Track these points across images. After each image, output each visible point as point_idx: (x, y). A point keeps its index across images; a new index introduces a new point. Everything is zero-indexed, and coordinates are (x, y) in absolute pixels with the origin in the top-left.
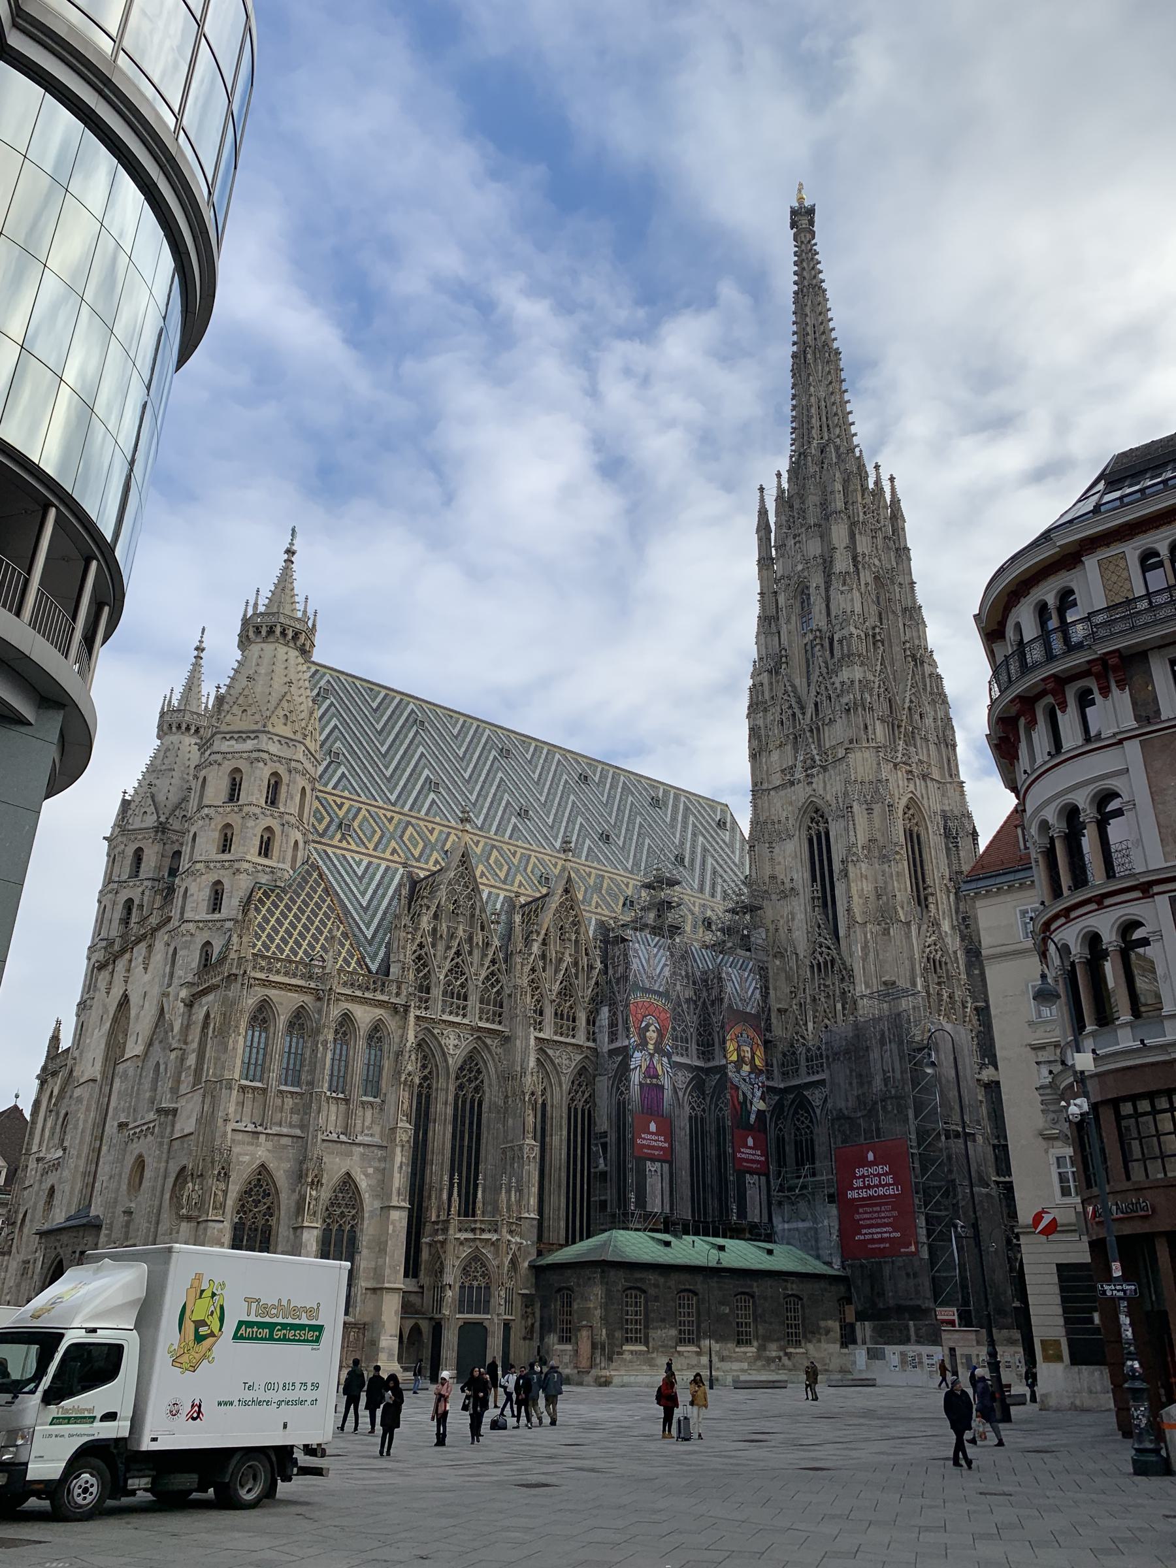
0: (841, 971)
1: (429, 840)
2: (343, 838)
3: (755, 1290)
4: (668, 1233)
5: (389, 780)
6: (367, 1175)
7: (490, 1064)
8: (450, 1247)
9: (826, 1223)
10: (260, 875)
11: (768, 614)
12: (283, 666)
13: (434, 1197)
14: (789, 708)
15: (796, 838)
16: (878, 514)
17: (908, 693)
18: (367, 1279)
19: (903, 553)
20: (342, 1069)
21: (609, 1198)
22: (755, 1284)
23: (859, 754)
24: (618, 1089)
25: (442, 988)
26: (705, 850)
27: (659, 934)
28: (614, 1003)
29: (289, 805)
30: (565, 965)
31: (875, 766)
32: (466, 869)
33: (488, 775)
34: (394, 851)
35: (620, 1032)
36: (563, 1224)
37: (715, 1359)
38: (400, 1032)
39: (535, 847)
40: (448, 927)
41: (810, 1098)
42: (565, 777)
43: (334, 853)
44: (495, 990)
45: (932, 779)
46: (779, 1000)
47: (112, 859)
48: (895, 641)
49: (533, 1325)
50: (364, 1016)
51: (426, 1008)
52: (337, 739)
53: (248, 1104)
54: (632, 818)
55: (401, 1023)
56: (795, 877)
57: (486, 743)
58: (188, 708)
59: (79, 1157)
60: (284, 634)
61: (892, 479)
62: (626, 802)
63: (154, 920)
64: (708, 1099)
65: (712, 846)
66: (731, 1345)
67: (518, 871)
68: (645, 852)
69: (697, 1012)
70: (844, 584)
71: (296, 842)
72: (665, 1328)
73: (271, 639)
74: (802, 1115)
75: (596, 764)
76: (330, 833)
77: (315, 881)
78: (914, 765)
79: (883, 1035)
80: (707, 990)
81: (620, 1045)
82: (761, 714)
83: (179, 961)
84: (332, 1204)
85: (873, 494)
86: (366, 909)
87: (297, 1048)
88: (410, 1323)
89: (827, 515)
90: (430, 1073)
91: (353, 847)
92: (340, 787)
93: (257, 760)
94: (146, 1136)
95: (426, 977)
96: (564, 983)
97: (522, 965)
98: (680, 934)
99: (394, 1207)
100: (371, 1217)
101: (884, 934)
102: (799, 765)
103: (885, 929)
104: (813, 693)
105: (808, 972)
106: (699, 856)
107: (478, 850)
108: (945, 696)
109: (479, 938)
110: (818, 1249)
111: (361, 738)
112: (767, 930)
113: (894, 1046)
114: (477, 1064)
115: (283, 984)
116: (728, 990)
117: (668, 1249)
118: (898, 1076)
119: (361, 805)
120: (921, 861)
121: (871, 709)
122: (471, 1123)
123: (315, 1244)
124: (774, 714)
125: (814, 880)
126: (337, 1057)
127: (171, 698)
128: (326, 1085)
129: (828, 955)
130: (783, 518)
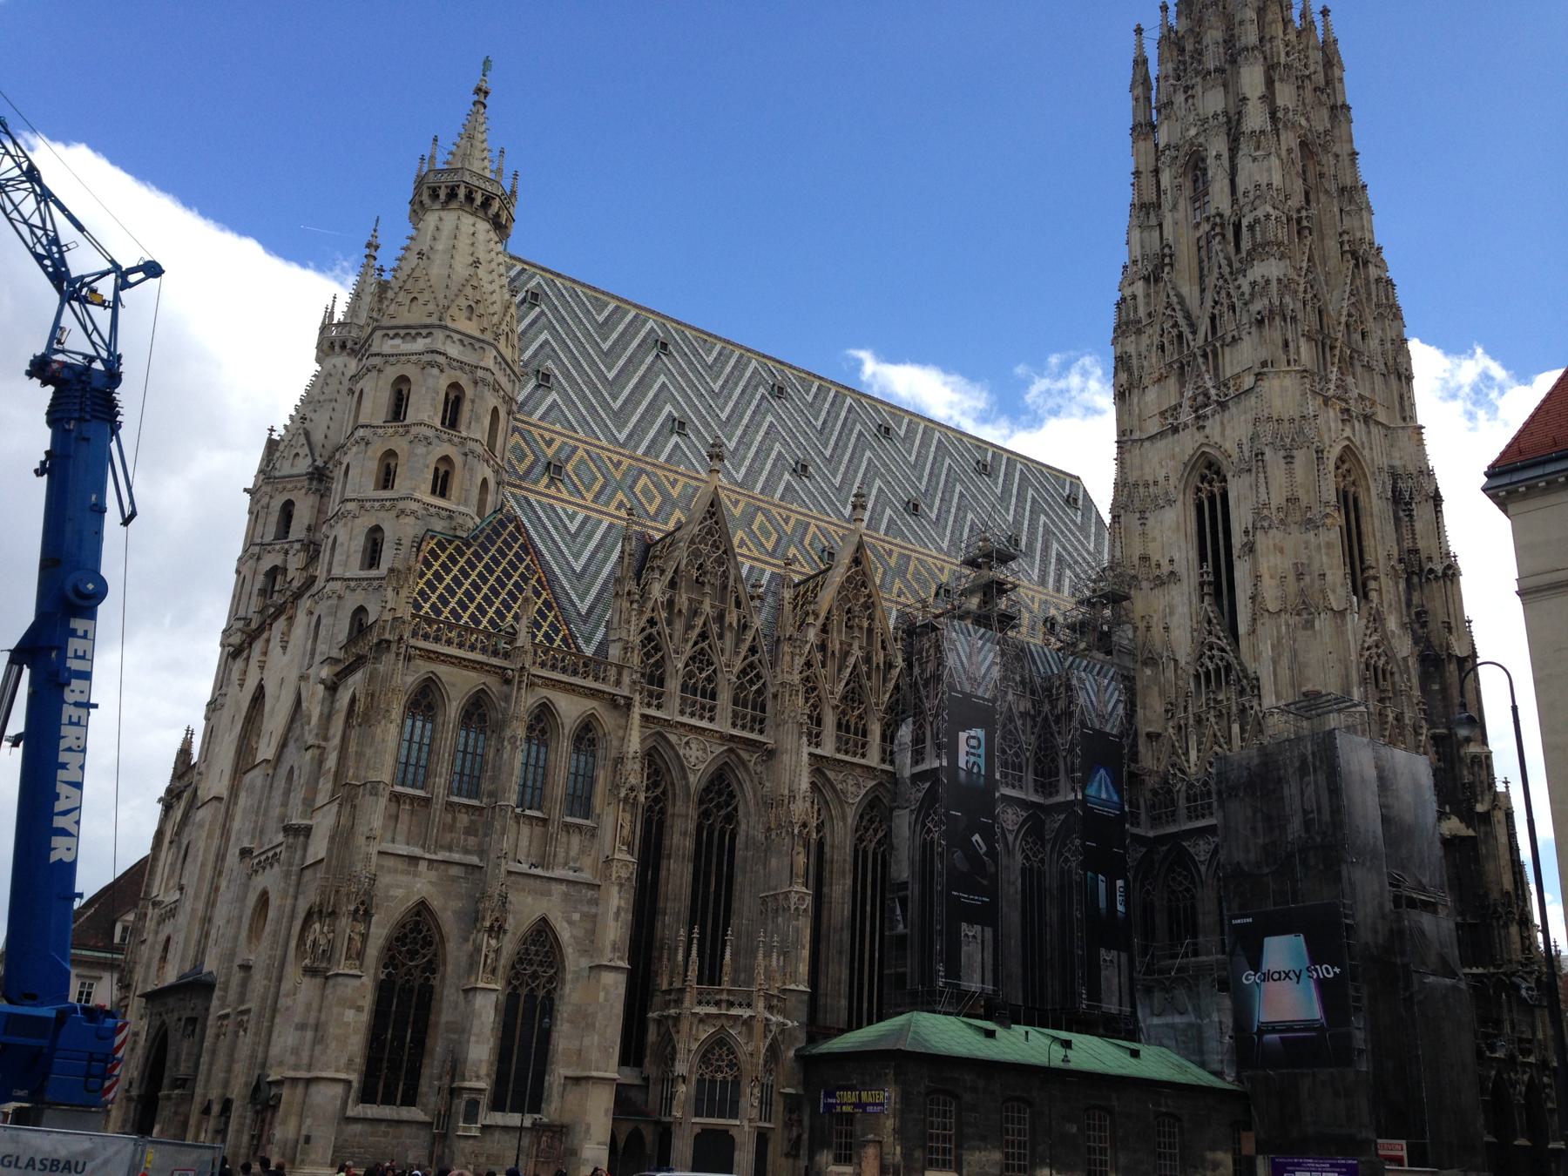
0: (1239, 680)
3: (1116, 1104)
4: (990, 1020)
6: (570, 923)
7: (747, 786)
8: (684, 1026)
9: (1215, 1017)
10: (434, 520)
11: (1146, 199)
13: (665, 956)
14: (1173, 327)
15: (1179, 504)
16: (1307, 57)
17: (1345, 304)
19: (1340, 111)
20: (539, 778)
21: (909, 970)
23: (1276, 383)
24: (924, 825)
25: (680, 681)
26: (1047, 530)
27: (988, 626)
28: (921, 713)
29: (475, 428)
30: (852, 660)
31: (1298, 397)
32: (716, 523)
34: (620, 505)
35: (928, 748)
36: (844, 1003)
38: (621, 733)
39: (815, 513)
40: (690, 600)
41: (1192, 850)
42: (858, 427)
43: (538, 502)
44: (754, 688)
45: (1377, 423)
46: (1148, 722)
47: (255, 514)
48: (1329, 232)
49: (799, 1137)
50: (570, 709)
51: (659, 707)
52: (549, 357)
53: (404, 817)
55: (623, 722)
57: (750, 378)
58: (355, 321)
59: (196, 897)
61: (1325, 12)
63: (296, 584)
64: (1048, 848)
65: (1057, 527)
67: (791, 541)
68: (967, 530)
69: (1036, 730)
70: (1258, 148)
71: (485, 482)
72: (985, 1150)
73: (454, 205)
74: (1180, 874)
76: (532, 476)
77: (511, 534)
78: (1352, 402)
79: (1304, 761)
80: (1050, 702)
81: (928, 767)
82: (1133, 337)
83: (322, 632)
84: (521, 961)
85: (1299, 34)
86: (580, 577)
87: (476, 747)
88: (626, 1128)
89: (1234, 54)
90: (664, 793)
91: (565, 495)
93: (431, 364)
94: (272, 865)
95: (660, 664)
96: (852, 684)
97: (793, 655)
98: (1014, 627)
99: (606, 966)
100: (576, 980)
101: (1305, 628)
102: (1186, 403)
103: (1307, 621)
104: (1209, 303)
105: (1192, 685)
106: (1040, 539)
107: (737, 512)
108: (1398, 309)
109: (732, 618)
110: (1201, 1052)
112: (1136, 629)
113: (1322, 778)
114: (729, 785)
115: (456, 657)
116: (1081, 701)
117: (989, 1042)
118: (1326, 817)
119: (577, 444)
120: (1359, 534)
121: (1294, 319)
122: (719, 864)
123: (492, 1013)
124: (1150, 336)
125: (1202, 558)
126: (532, 761)
128: (512, 799)
129: (1222, 659)
130: (1170, 66)
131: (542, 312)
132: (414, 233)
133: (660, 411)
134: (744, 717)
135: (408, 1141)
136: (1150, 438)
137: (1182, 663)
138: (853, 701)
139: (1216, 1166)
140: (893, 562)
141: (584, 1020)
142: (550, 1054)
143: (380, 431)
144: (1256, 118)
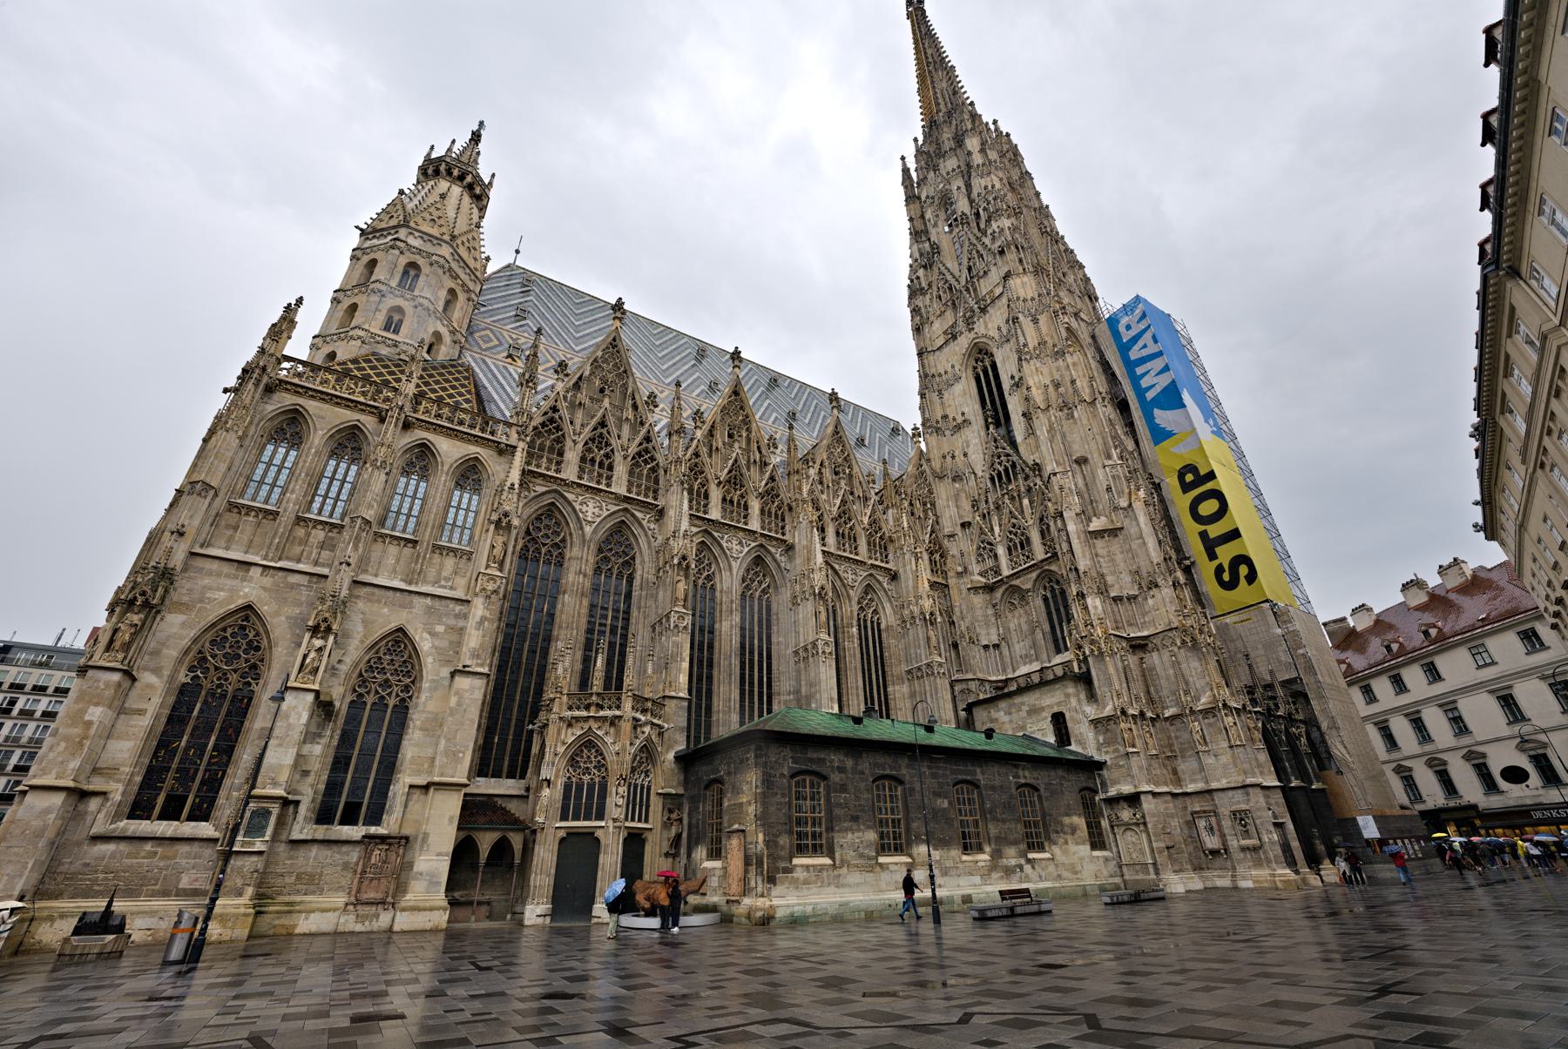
2: (510, 356)
3: (980, 777)
6: (432, 634)
7: (642, 541)
8: (552, 730)
11: (919, 229)
18: (418, 772)
22: (978, 770)
23: (1018, 281)
37: (936, 872)
49: (679, 836)
56: (966, 410)
66: (955, 853)
72: (859, 830)
93: (392, 247)
100: (434, 689)
104: (965, 261)
105: (989, 485)
134: (639, 486)
135: (184, 862)
136: (940, 348)
137: (980, 474)
138: (735, 484)
139: (1074, 830)
141: (435, 725)
142: (398, 763)
144: (977, 159)
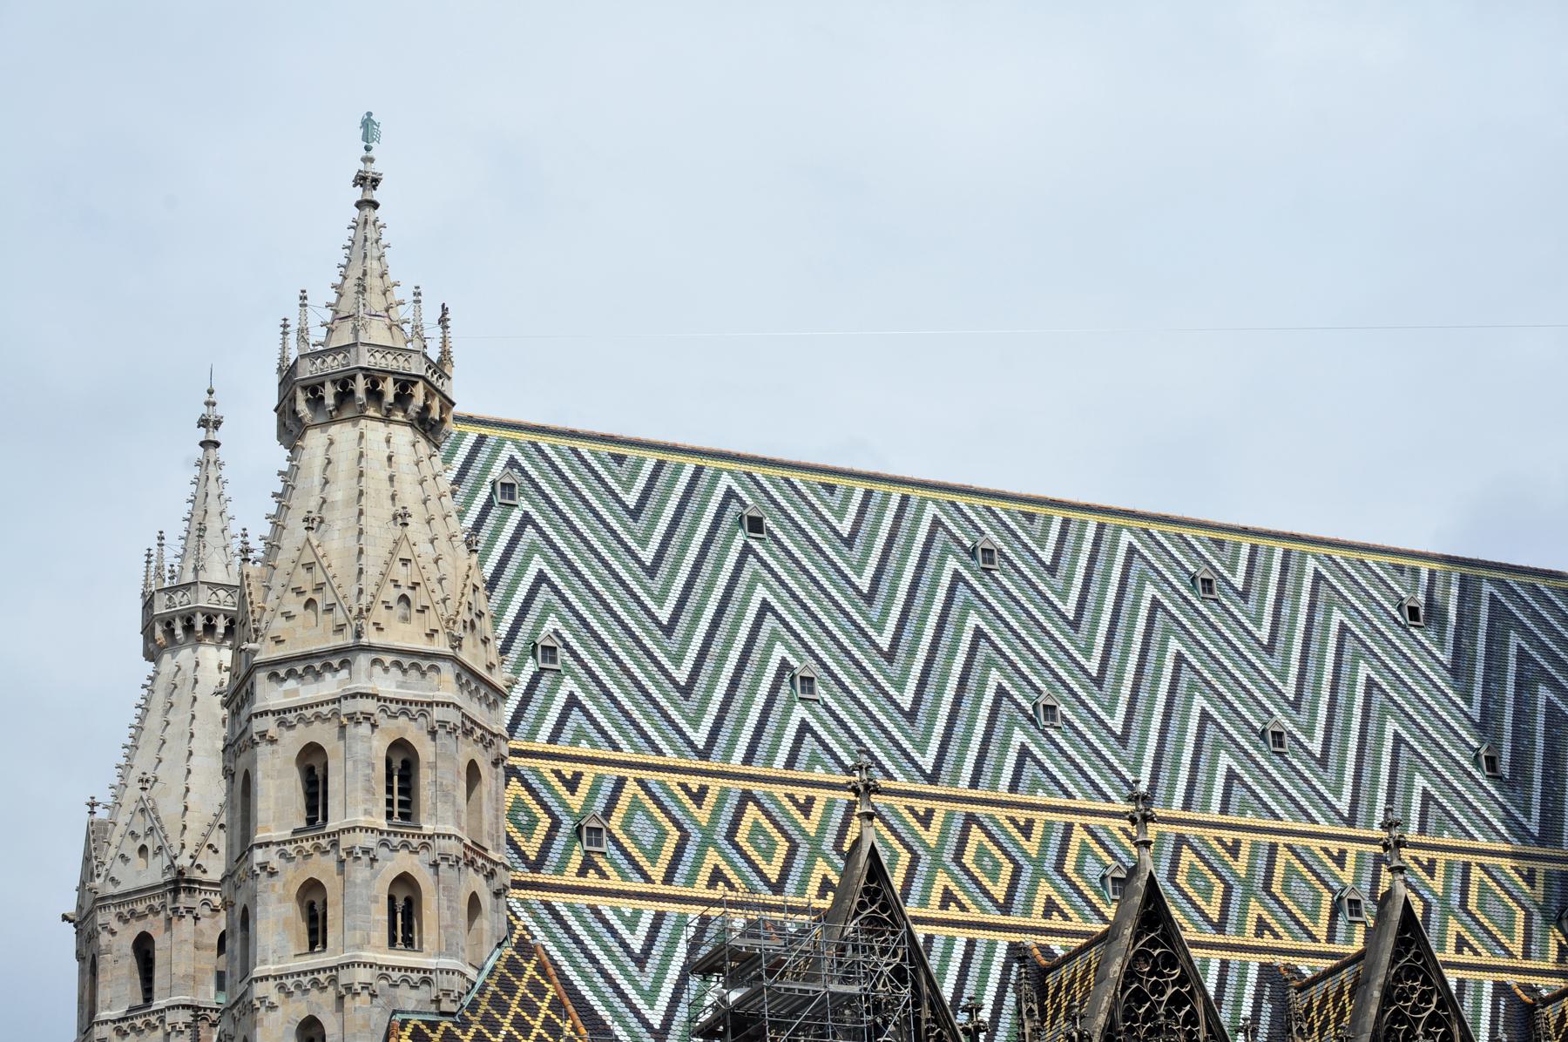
1: (803, 832)
2: (587, 865)
5: (686, 691)
10: (398, 991)
12: (385, 474)
32: (884, 908)
33: (940, 628)
34: (716, 876)
39: (1080, 802)
42: (1150, 591)
43: (570, 907)
52: (548, 608)
54: (1346, 669)
60: (374, 394)
62: (1326, 628)
67: (1039, 873)
68: (1386, 759)
73: (347, 414)
75: (1236, 538)
76: (554, 856)
91: (615, 883)
92: (567, 733)
106: (1540, 742)
111: (607, 596)
119: (623, 772)
127: (161, 556)
131: (526, 515)
132: (285, 467)
133: (764, 662)
140: (1241, 867)
143: (289, 848)
